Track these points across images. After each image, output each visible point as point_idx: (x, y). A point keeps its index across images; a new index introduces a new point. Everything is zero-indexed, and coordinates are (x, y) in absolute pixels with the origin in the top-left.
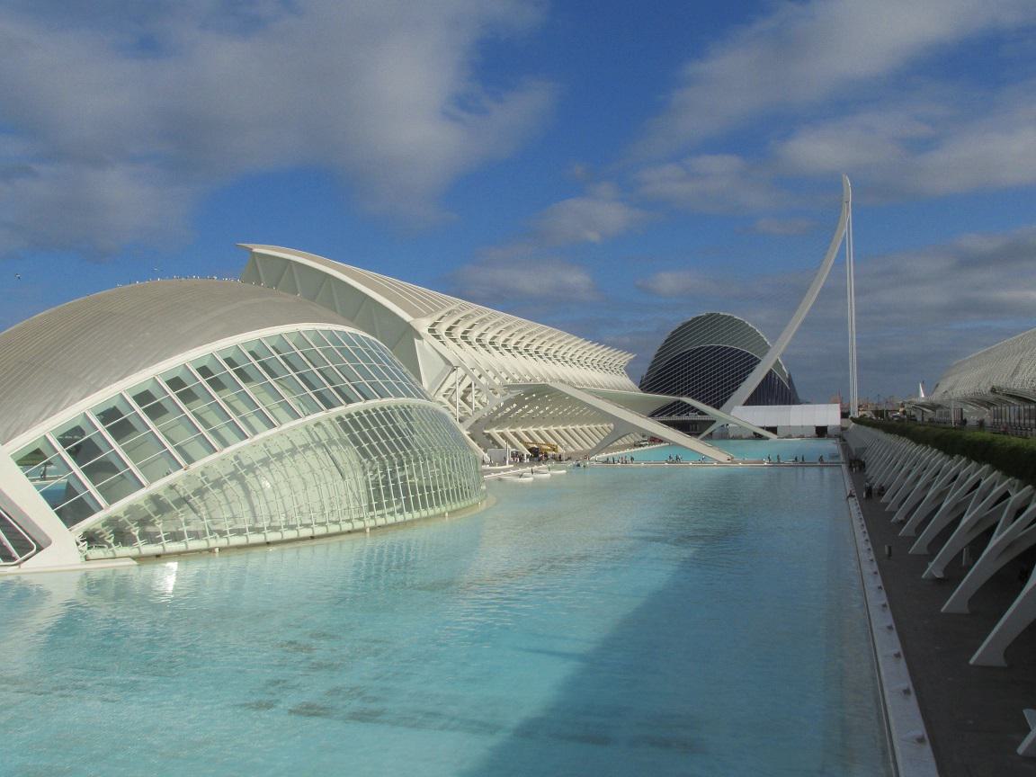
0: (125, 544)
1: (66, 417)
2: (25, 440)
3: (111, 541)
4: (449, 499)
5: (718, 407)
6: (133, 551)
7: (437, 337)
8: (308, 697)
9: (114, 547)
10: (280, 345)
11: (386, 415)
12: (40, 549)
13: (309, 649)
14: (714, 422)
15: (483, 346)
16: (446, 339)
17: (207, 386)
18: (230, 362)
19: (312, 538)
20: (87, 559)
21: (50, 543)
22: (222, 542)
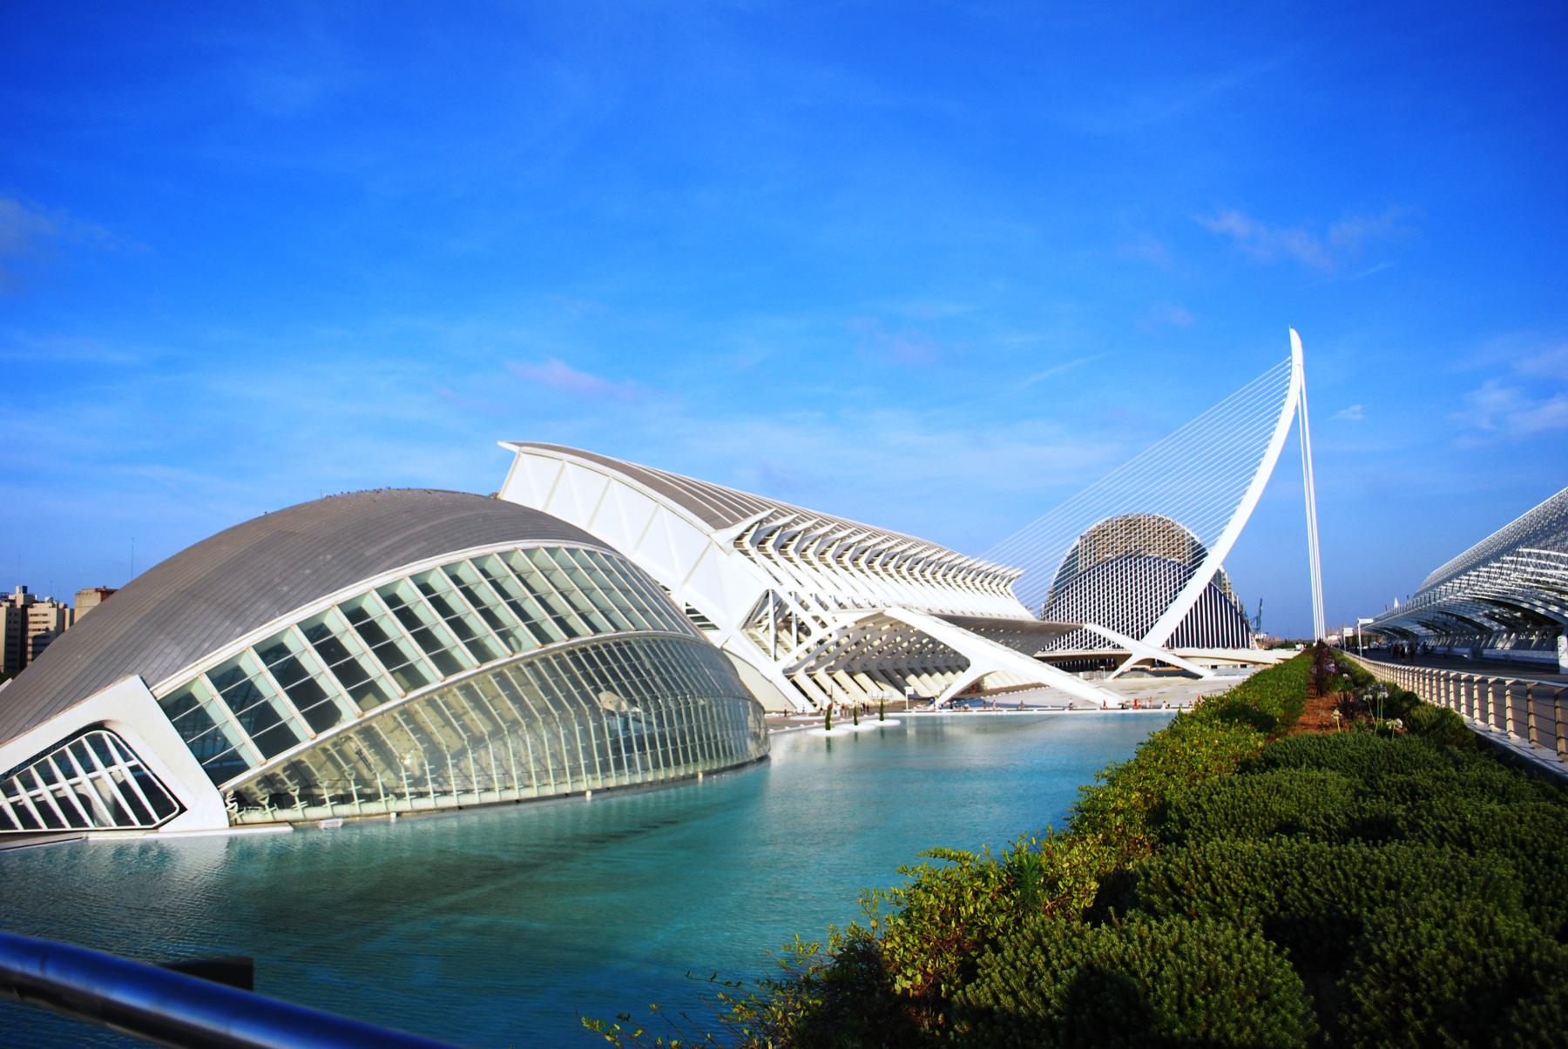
0: (282, 807)
3: (265, 802)
4: (703, 755)
12: (183, 809)
14: (1127, 657)
19: (518, 802)
20: (233, 824)
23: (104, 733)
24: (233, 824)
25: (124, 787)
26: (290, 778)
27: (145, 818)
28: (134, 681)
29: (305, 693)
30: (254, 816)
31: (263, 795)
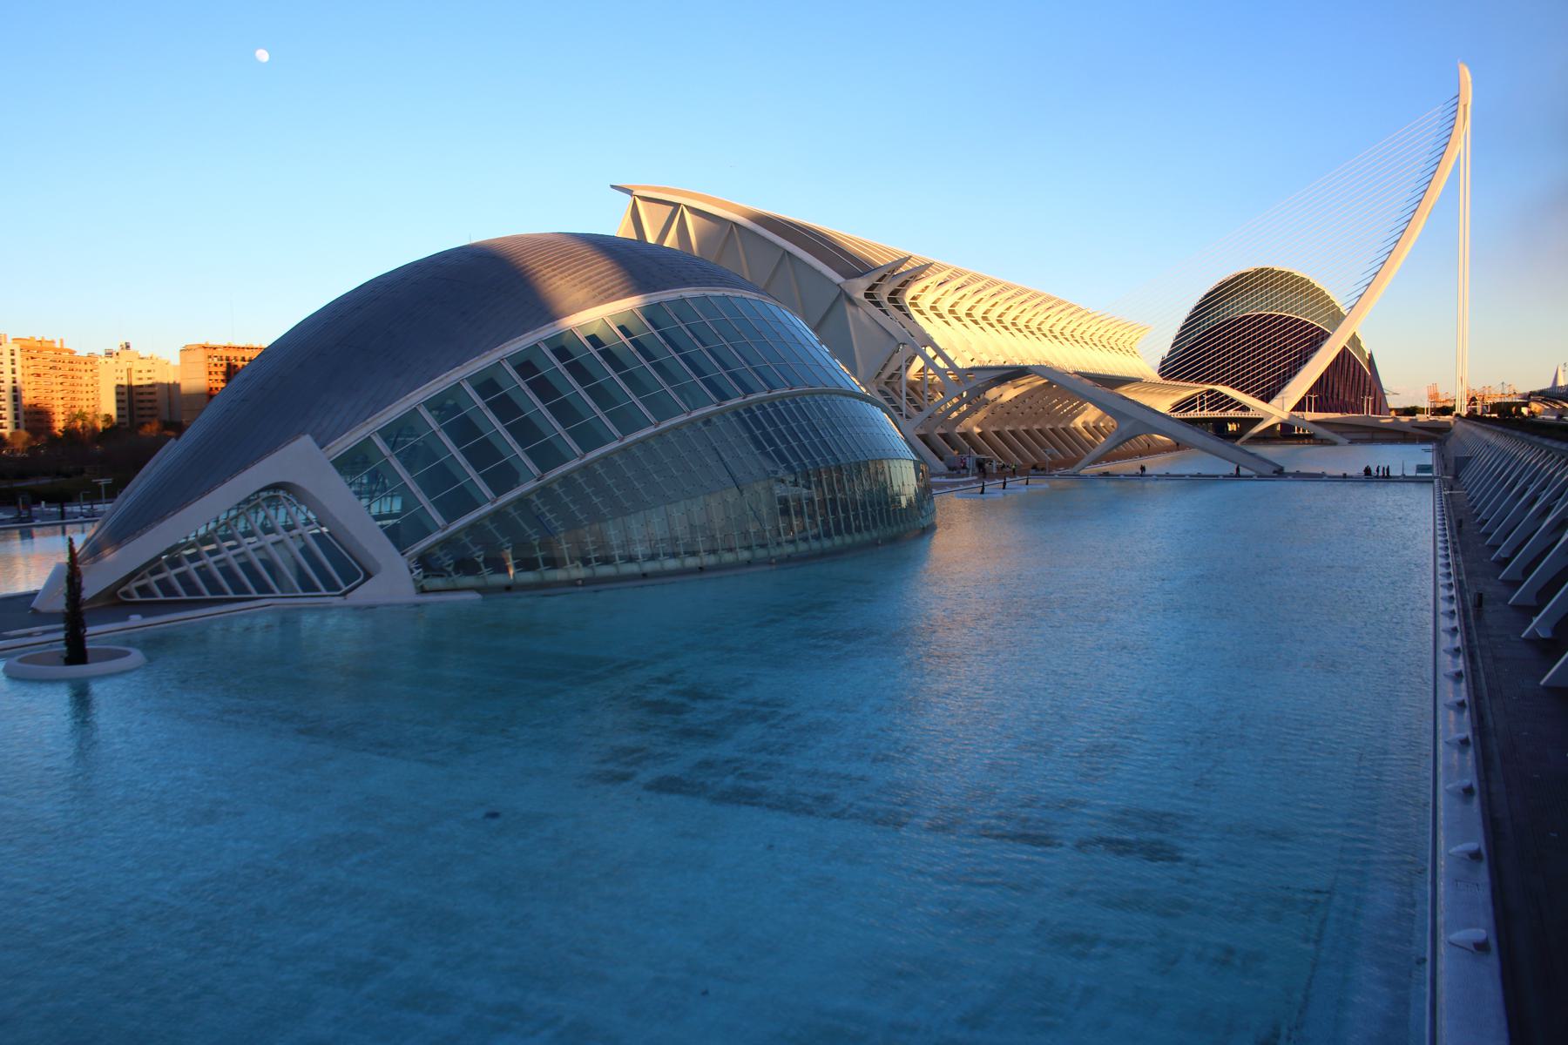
0: (468, 573)
4: (882, 521)
7: (877, 304)
8: (673, 769)
9: (455, 576)
12: (368, 576)
13: (678, 710)
14: (1260, 420)
17: (565, 372)
19: (701, 569)
24: (422, 590)
25: (306, 551)
27: (331, 586)
28: (306, 442)
29: (483, 453)
30: (438, 583)
31: (448, 562)
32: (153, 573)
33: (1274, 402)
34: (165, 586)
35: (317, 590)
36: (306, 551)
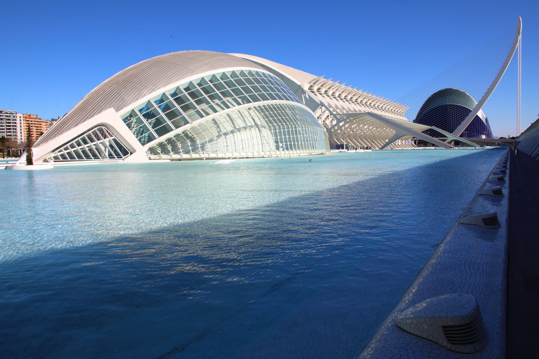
1: (141, 102)
2: (126, 111)
5: (451, 132)
6: (169, 157)
7: (313, 92)
10: (234, 74)
11: (281, 107)
12: (131, 153)
15: (335, 98)
16: (317, 93)
18: (211, 81)
21: (135, 151)
22: (206, 156)
23: (103, 127)
25: (111, 146)
26: (168, 144)
27: (119, 157)
28: (111, 110)
32: (59, 152)
33: (454, 132)
34: (63, 156)
35: (114, 158)
36: (111, 146)
